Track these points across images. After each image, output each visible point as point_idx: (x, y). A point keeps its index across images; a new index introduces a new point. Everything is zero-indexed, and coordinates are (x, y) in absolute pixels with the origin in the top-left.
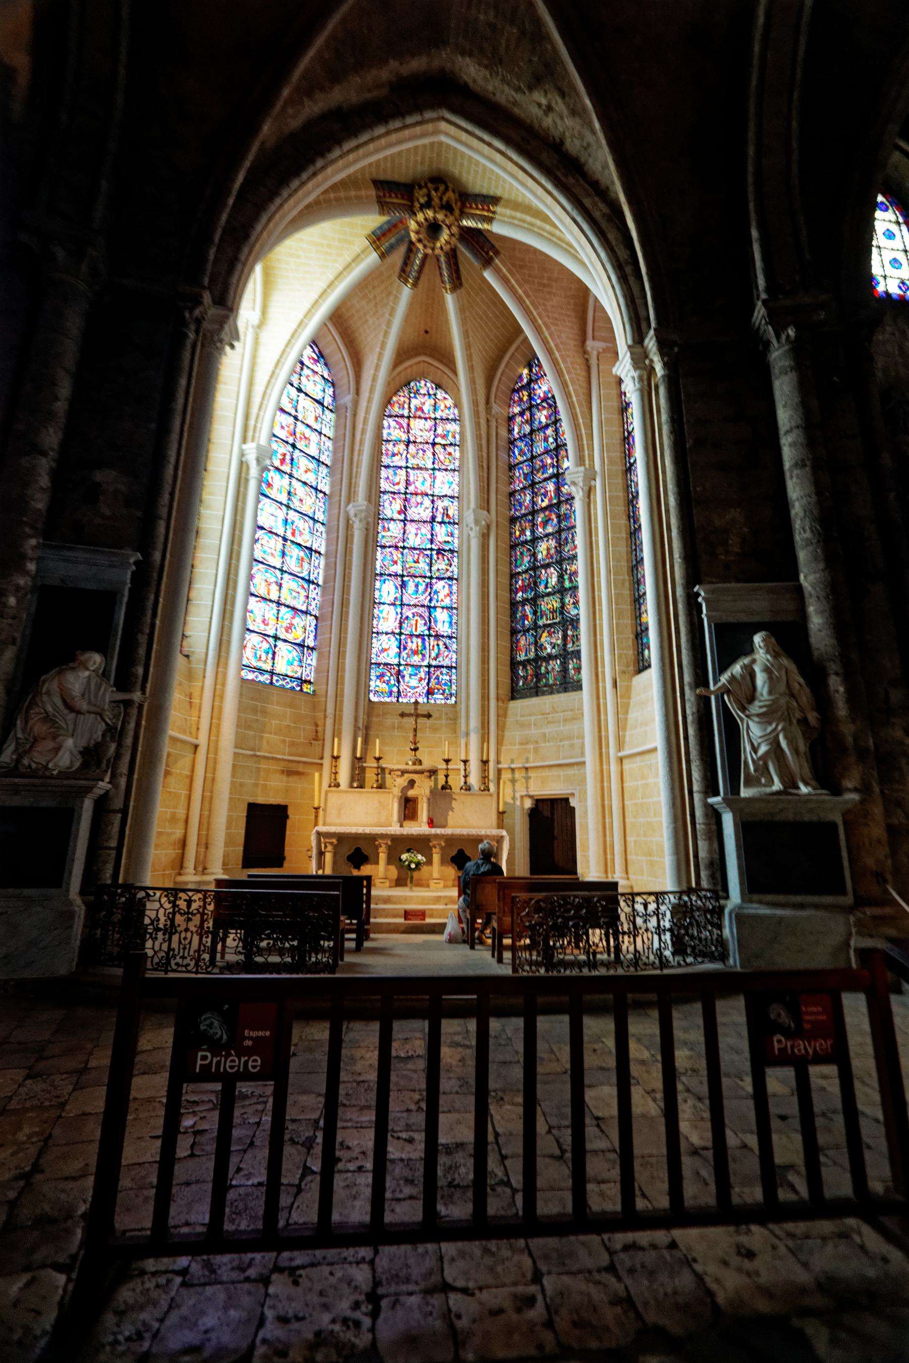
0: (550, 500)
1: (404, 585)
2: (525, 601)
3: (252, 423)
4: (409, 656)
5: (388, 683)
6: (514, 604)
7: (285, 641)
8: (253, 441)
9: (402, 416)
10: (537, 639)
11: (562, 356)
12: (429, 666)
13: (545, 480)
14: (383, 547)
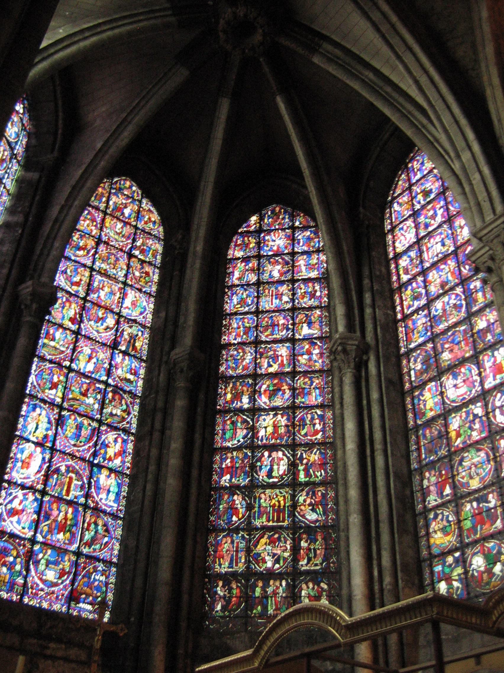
1: (60, 422)
12: (78, 554)
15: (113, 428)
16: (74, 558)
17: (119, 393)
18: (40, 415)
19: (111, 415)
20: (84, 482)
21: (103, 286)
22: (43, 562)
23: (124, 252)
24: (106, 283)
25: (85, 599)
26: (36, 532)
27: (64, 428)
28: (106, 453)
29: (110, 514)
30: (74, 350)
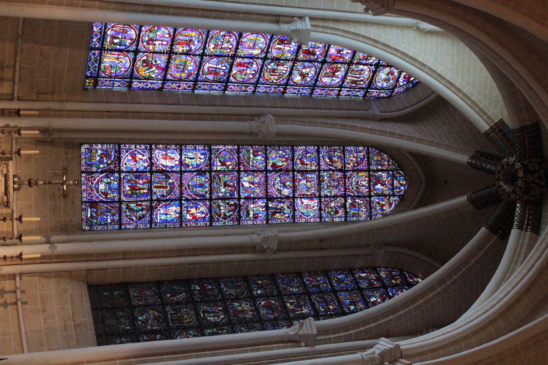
0: (294, 311)
1: (200, 172)
2: (190, 293)
3: (330, 25)
4: (129, 181)
5: (101, 162)
6: (187, 282)
7: (135, 60)
8: (312, 26)
9: (369, 164)
10: (152, 306)
11: (420, 305)
12: (120, 202)
13: (313, 305)
14: (238, 152)
15: (210, 209)
16: (116, 200)
17: (236, 208)
18: (200, 158)
19: (219, 206)
20: (166, 196)
21: (310, 182)
22: (109, 180)
23: (345, 191)
24: (313, 183)
25: (93, 211)
26: (125, 172)
27: (198, 176)
28: (192, 207)
29: (151, 218)
30: (254, 171)
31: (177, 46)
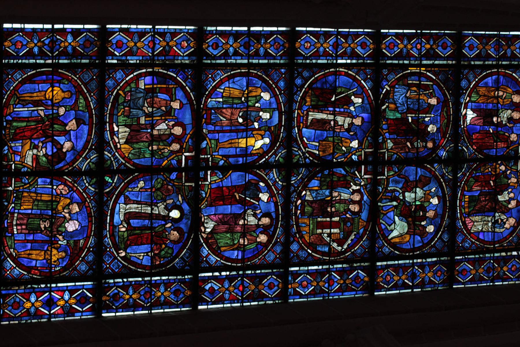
31: (17, 145)
